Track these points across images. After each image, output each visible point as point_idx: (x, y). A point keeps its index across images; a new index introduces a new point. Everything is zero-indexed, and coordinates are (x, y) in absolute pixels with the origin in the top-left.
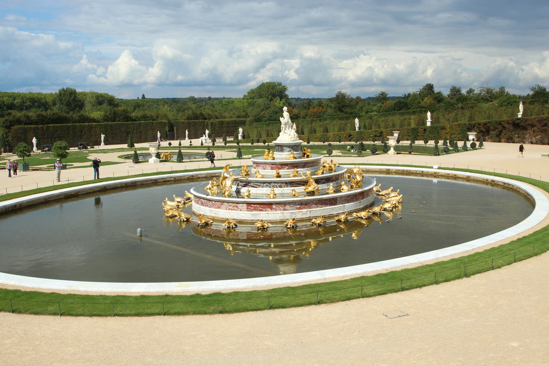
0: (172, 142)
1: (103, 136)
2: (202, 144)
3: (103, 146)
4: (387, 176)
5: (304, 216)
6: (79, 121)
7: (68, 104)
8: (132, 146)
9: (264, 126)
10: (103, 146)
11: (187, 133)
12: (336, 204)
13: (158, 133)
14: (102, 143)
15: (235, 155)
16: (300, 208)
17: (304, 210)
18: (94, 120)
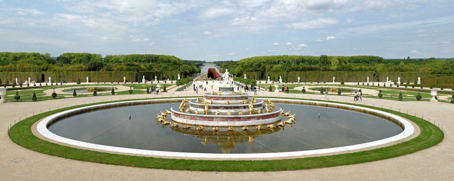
0: (374, 83)
1: (334, 78)
2: (391, 85)
3: (334, 83)
4: (364, 114)
5: (192, 123)
6: (323, 70)
7: (323, 63)
8: (343, 83)
9: (436, 77)
10: (334, 83)
11: (387, 78)
12: (213, 121)
13: (368, 78)
14: (334, 81)
15: (320, 92)
16: (191, 119)
17: (193, 120)
18: (331, 70)
